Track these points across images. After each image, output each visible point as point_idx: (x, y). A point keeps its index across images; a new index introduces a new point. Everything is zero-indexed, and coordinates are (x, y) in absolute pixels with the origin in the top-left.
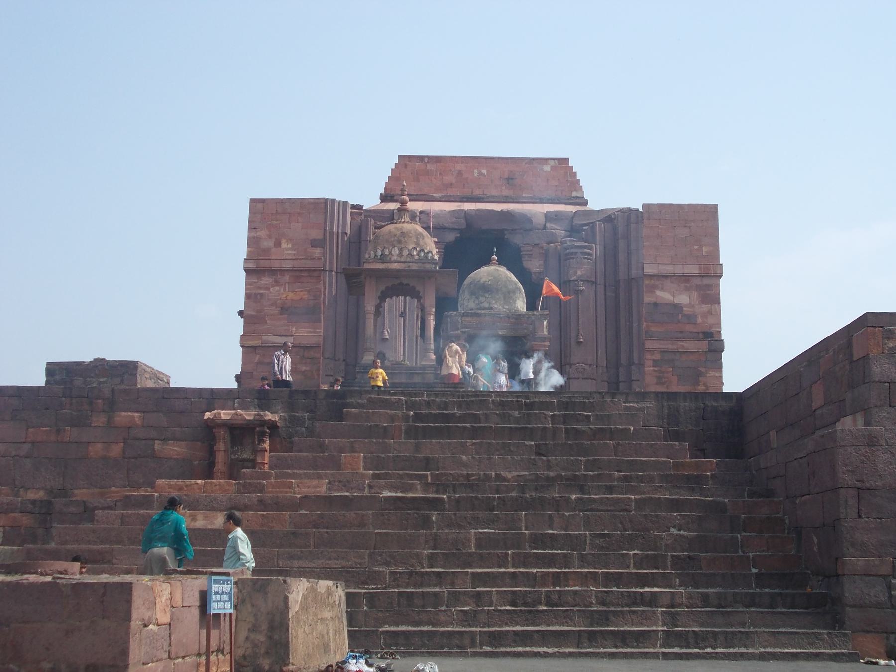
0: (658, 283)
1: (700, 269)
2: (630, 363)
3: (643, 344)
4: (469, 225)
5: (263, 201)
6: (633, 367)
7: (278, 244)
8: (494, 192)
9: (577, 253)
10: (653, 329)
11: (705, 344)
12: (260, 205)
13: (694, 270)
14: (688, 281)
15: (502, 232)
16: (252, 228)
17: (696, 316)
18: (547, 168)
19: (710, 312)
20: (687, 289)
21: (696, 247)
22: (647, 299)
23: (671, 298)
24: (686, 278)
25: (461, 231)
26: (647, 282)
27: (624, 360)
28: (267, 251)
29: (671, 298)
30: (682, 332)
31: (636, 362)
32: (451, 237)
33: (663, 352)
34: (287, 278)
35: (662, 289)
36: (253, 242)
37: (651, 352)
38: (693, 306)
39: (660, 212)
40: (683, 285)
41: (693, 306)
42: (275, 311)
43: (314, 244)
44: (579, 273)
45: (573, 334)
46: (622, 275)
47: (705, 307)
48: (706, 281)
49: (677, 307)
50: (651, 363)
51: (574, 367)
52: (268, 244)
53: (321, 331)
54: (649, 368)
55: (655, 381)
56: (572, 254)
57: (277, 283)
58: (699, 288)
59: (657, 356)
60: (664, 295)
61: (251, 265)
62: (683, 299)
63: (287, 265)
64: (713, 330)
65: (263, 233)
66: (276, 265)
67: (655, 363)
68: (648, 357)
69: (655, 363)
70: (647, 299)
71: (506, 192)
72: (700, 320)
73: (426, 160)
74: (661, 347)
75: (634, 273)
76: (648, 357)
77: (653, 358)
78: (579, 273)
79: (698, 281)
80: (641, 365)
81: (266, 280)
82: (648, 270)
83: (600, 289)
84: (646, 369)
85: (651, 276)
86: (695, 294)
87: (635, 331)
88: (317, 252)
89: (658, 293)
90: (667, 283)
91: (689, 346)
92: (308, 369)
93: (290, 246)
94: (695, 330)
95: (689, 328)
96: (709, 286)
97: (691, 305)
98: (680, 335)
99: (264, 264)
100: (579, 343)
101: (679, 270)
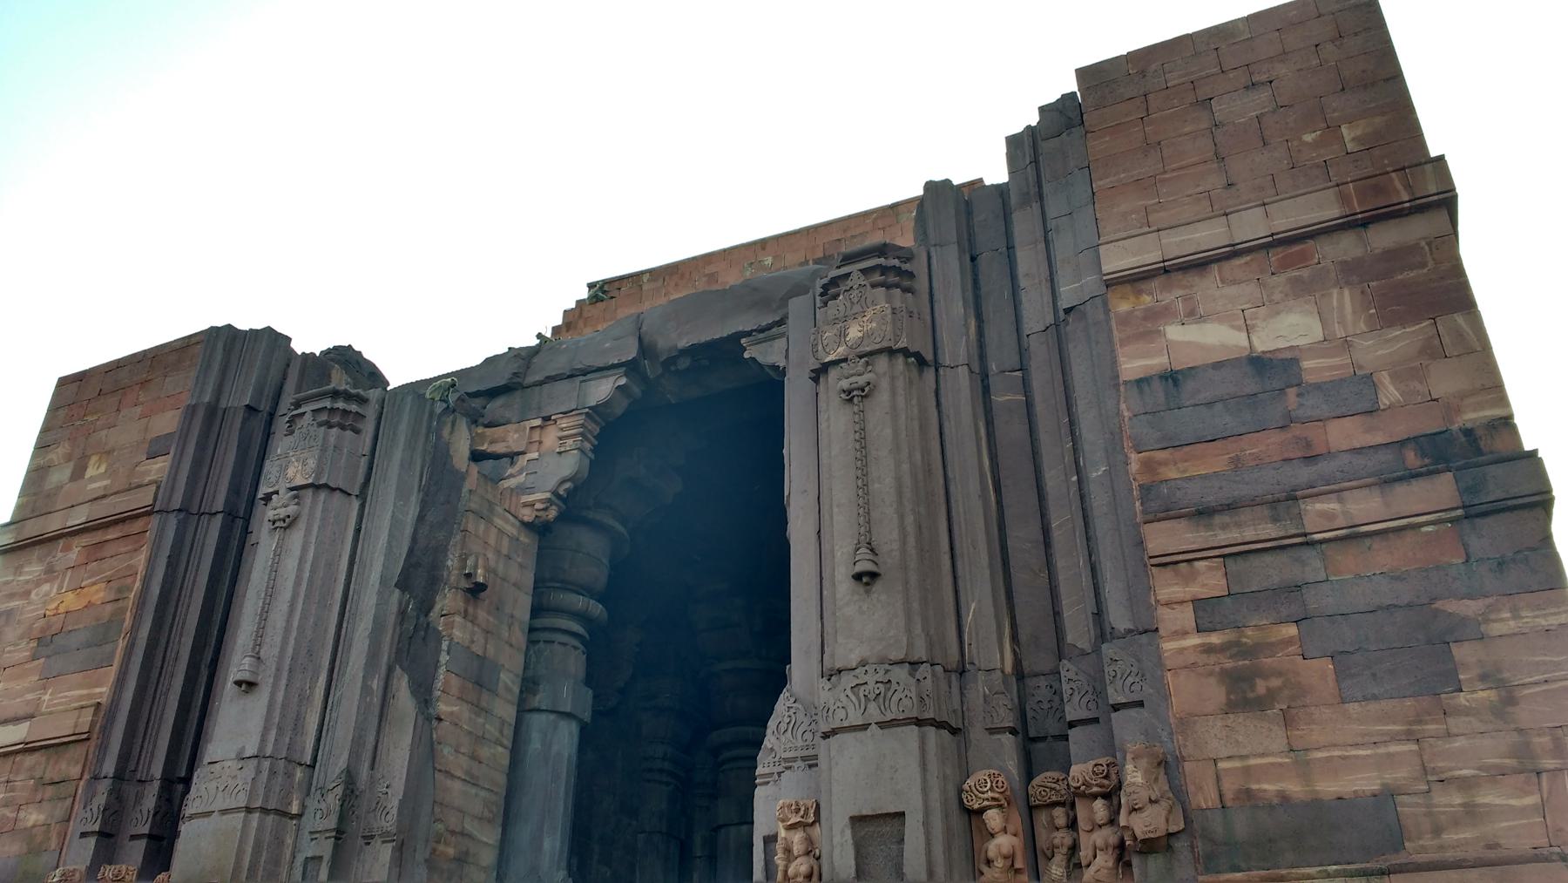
0: (1168, 298)
1: (1344, 199)
2: (1103, 634)
3: (1140, 543)
4: (646, 349)
6: (1108, 650)
9: (848, 275)
10: (1172, 473)
11: (1441, 491)
17: (1369, 381)
20: (1301, 289)
21: (1308, 138)
22: (1133, 365)
23: (1240, 339)
26: (1124, 307)
27: (1078, 632)
29: (1240, 339)
30: (1310, 459)
31: (1119, 618)
32: (601, 390)
34: (74, 555)
35: (1193, 315)
38: (1346, 344)
41: (1346, 344)
44: (854, 332)
46: (1036, 314)
47: (1404, 339)
48: (1384, 237)
50: (1185, 617)
51: (848, 680)
53: (103, 691)
54: (1180, 640)
55: (1216, 694)
58: (1351, 272)
59: (1210, 581)
60: (1205, 334)
62: (1291, 328)
64: (1472, 416)
67: (1207, 613)
69: (1207, 613)
72: (1389, 393)
73: (646, 278)
74: (1223, 537)
76: (1168, 587)
77: (1196, 590)
78: (854, 332)
79: (1347, 247)
83: (960, 385)
84: (1168, 646)
85: (1136, 279)
86: (1344, 300)
87: (1099, 501)
88: (158, 468)
89: (1174, 332)
90: (1208, 287)
91: (1365, 507)
93: (102, 469)
94: (1379, 438)
98: (1304, 474)
101: (1251, 226)
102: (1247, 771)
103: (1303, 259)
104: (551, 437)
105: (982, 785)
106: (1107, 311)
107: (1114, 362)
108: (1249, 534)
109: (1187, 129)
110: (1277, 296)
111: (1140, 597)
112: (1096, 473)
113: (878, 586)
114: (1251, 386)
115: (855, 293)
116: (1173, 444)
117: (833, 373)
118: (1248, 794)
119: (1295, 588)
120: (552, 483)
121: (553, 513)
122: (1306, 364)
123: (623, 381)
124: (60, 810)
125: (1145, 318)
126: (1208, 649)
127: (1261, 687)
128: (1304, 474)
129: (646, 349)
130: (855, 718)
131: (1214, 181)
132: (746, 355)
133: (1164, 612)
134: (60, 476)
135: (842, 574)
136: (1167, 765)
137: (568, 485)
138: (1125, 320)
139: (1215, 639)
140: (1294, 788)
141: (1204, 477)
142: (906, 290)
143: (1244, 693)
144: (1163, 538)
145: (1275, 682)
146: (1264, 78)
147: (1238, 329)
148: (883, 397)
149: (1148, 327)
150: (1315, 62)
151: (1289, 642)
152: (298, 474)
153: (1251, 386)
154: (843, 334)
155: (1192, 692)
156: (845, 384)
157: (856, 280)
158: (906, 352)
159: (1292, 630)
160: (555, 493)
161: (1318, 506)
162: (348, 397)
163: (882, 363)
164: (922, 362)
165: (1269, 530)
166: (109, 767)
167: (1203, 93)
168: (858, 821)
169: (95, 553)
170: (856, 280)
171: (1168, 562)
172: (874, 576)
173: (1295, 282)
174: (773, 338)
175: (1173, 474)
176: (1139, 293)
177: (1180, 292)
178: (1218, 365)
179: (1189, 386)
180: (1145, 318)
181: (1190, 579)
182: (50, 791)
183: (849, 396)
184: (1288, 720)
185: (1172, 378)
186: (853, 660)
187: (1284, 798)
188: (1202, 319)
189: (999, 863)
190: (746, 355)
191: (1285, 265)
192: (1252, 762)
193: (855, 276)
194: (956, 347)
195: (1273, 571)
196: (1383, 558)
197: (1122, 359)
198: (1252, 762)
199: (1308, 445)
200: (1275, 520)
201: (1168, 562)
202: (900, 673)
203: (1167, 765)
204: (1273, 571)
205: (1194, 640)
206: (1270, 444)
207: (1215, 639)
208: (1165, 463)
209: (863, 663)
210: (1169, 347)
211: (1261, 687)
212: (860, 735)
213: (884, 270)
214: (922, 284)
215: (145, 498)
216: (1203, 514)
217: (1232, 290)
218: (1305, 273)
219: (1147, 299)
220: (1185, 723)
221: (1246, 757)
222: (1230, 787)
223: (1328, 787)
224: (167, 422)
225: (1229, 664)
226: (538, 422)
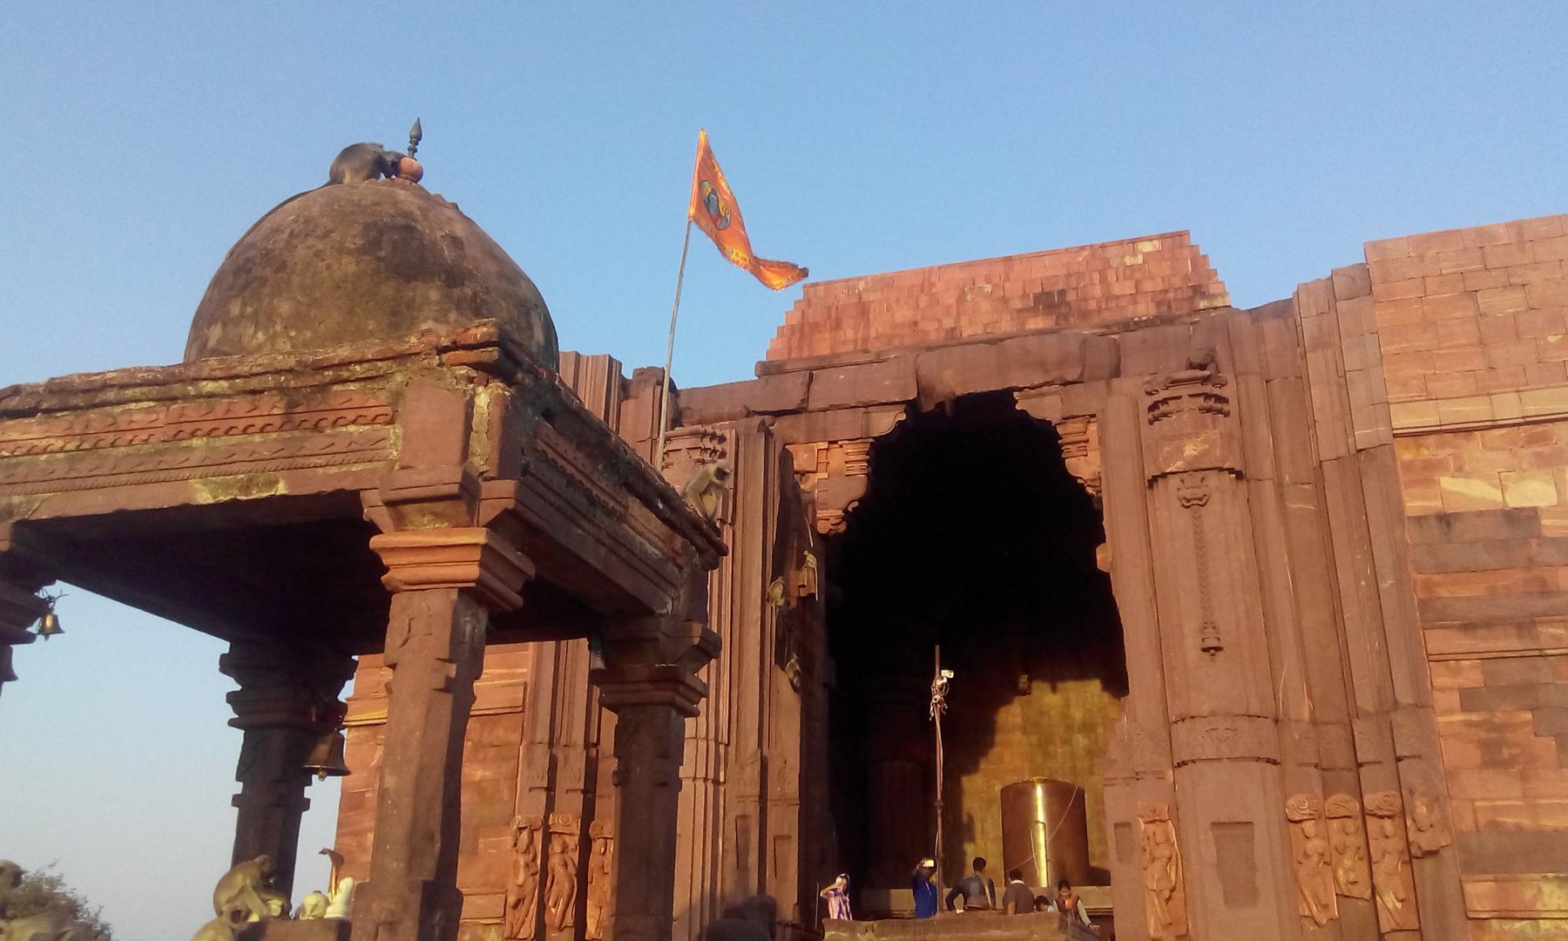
0: (1442, 454)
4: (923, 391)
6: (1398, 718)
15: (1004, 398)
21: (1552, 339)
22: (1415, 504)
26: (1406, 455)
27: (1366, 700)
32: (885, 422)
33: (1486, 658)
35: (1460, 471)
39: (1421, 257)
40: (1527, 452)
45: (1190, 627)
49: (1522, 520)
50: (1455, 700)
54: (1450, 717)
55: (1475, 756)
56: (1165, 401)
59: (1471, 675)
60: (1472, 488)
67: (1469, 700)
68: (1441, 678)
69: (1469, 700)
75: (1363, 435)
76: (1441, 678)
78: (1190, 450)
80: (1422, 706)
82: (1405, 419)
85: (1417, 435)
87: (1388, 604)
89: (1447, 483)
90: (1473, 449)
92: (488, 774)
98: (1540, 605)
101: (1508, 407)
102: (1494, 809)
103: (1543, 439)
104: (837, 457)
105: (1299, 804)
106: (1394, 460)
107: (1400, 501)
108: (1502, 645)
109: (1458, 314)
110: (1525, 466)
111: (1419, 683)
112: (1387, 584)
113: (1220, 655)
114: (1504, 533)
115: (1185, 416)
116: (1443, 569)
117: (1174, 482)
118: (1494, 825)
120: (843, 504)
121: (842, 528)
122: (1545, 522)
123: (903, 417)
124: (506, 769)
125: (1424, 468)
126: (1469, 724)
127: (1506, 753)
128: (1540, 605)
129: (923, 391)
130: (1210, 753)
131: (1478, 363)
132: (1018, 407)
133: (1437, 695)
135: (1192, 645)
137: (856, 504)
138: (1408, 467)
139: (1474, 717)
140: (1526, 822)
141: (1468, 599)
142: (1227, 414)
144: (1438, 641)
145: (1515, 751)
146: (1519, 281)
147: (1494, 486)
148: (1214, 506)
149: (1427, 473)
150: (1559, 275)
151: (1526, 723)
153: (1504, 533)
154: (1180, 450)
155: (1456, 752)
156: (1188, 493)
157: (1186, 403)
158: (1231, 471)
159: (1528, 716)
160: (845, 511)
161: (1551, 630)
162: (713, 436)
163: (1213, 480)
164: (1239, 476)
165: (1514, 644)
166: (543, 734)
167: (1471, 284)
168: (1217, 825)
170: (1186, 403)
171: (1442, 659)
172: (1218, 649)
173: (1538, 455)
174: (1042, 395)
175: (1445, 594)
176: (1419, 447)
177: (1451, 451)
178: (1480, 514)
179: (1457, 527)
180: (1424, 468)
181: (1457, 672)
182: (492, 752)
183: (1187, 503)
184: (1524, 777)
185: (1445, 520)
186: (1205, 709)
187: (1519, 827)
188: (1467, 476)
189: (1315, 858)
190: (1018, 407)
191: (1532, 440)
192: (1499, 803)
193: (1185, 399)
197: (1406, 498)
198: (1499, 803)
199: (1543, 582)
200: (1520, 636)
201: (1442, 659)
202: (1243, 724)
204: (1514, 672)
205: (1460, 717)
207: (1474, 717)
208: (1437, 585)
209: (1213, 714)
210: (1443, 495)
211: (1506, 753)
212: (1216, 764)
213: (1207, 396)
214: (1232, 407)
216: (1468, 627)
217: (1490, 455)
218: (1546, 449)
219: (1425, 452)
220: (1451, 775)
221: (1494, 800)
222: (1483, 818)
223: (1549, 823)
225: (1483, 735)
226: (825, 445)
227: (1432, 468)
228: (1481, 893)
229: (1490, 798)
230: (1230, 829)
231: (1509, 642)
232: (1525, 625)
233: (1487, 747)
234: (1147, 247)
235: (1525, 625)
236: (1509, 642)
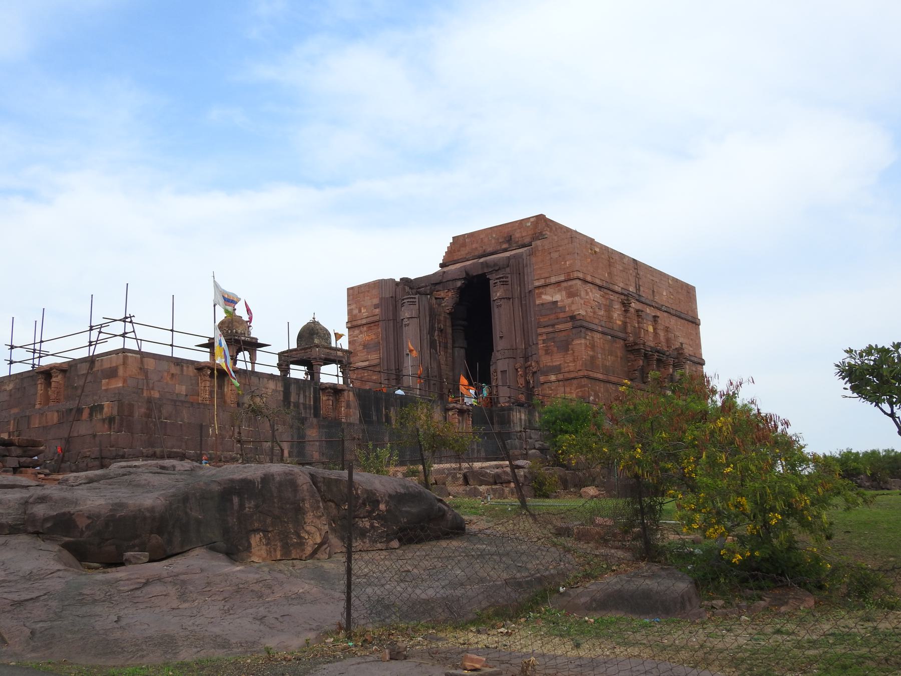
4: (467, 274)
5: (352, 288)
7: (360, 311)
8: (499, 248)
11: (570, 325)
12: (351, 291)
13: (562, 278)
14: (559, 286)
16: (349, 305)
18: (529, 224)
19: (573, 303)
20: (560, 291)
22: (538, 302)
24: (558, 283)
25: (464, 279)
28: (355, 316)
32: (459, 284)
34: (365, 329)
36: (350, 312)
37: (541, 334)
42: (361, 348)
43: (376, 306)
47: (570, 300)
48: (570, 283)
52: (356, 312)
57: (361, 332)
59: (544, 337)
60: (547, 298)
61: (349, 325)
62: (557, 297)
63: (364, 321)
65: (353, 307)
66: (359, 322)
70: (538, 302)
71: (504, 246)
79: (564, 285)
81: (357, 332)
82: (537, 284)
85: (539, 287)
86: (564, 293)
88: (377, 311)
89: (543, 297)
90: (548, 289)
95: (561, 315)
96: (571, 286)
97: (562, 301)
99: (355, 323)
100: (501, 337)
104: (450, 294)
105: (518, 365)
119: (554, 338)
128: (556, 321)
129: (467, 274)
134: (356, 312)
136: (537, 362)
143: (547, 352)
152: (407, 315)
155: (542, 352)
169: (369, 329)
185: (542, 304)
194: (516, 294)
195: (551, 336)
196: (564, 333)
203: (537, 362)
206: (553, 317)
215: (377, 318)
224: (376, 301)
227: (541, 293)
228: (542, 379)
229: (546, 361)
230: (504, 372)
231: (550, 329)
232: (553, 326)
233: (546, 351)
234: (532, 220)
235: (553, 326)
236: (550, 329)
